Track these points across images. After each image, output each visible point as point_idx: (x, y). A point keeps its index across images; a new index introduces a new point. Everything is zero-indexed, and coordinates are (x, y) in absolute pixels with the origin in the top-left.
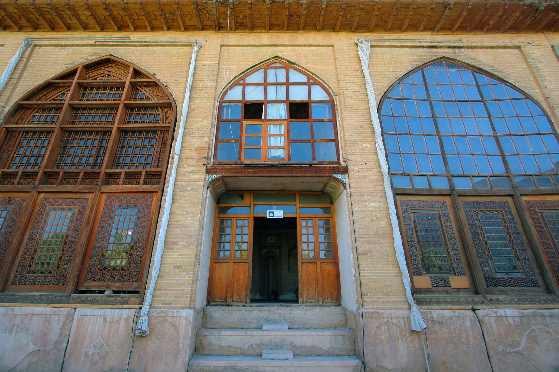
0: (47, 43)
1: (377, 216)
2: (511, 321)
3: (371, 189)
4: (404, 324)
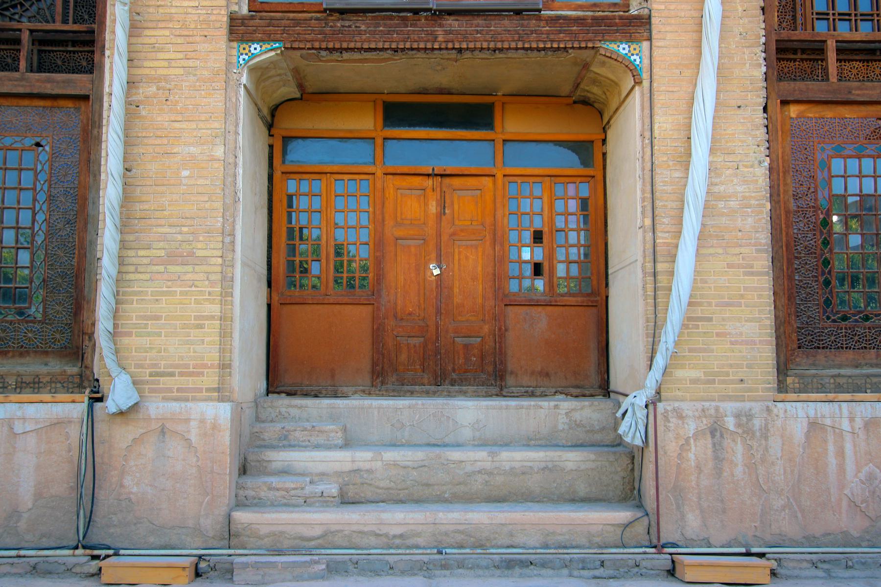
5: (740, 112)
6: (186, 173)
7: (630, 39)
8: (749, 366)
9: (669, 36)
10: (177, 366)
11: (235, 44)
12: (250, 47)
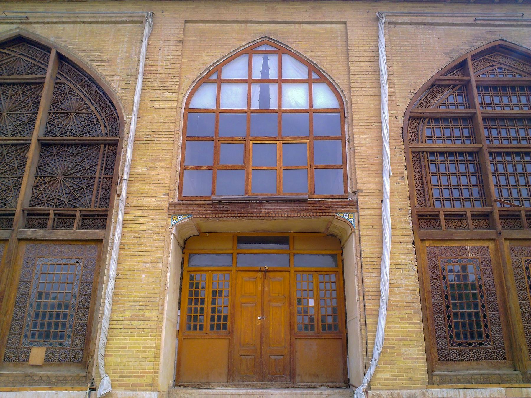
0: (406, 19)
5: (401, 245)
6: (144, 276)
7: (349, 212)
8: (413, 371)
9: (366, 210)
10: (132, 373)
11: (171, 216)
12: (177, 217)
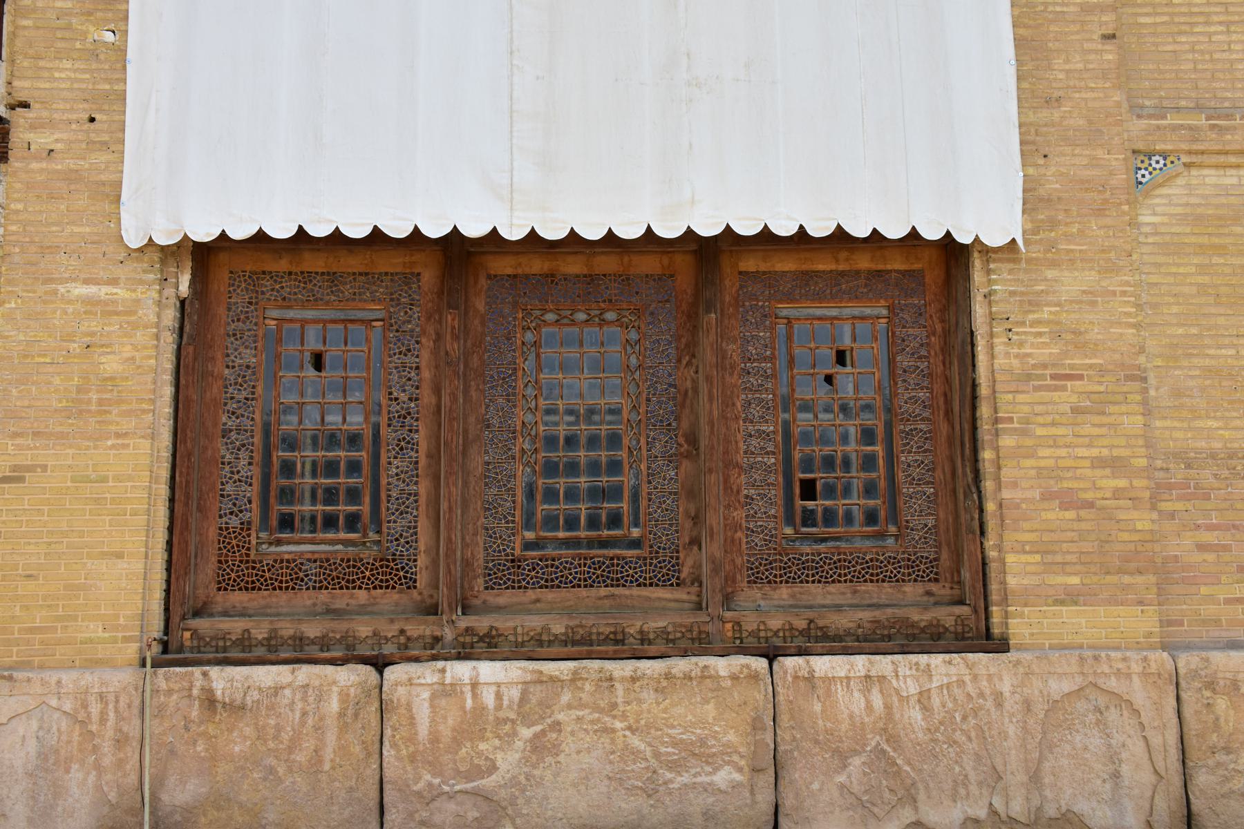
1: (93, 334)
2: (489, 698)
3: (88, 230)
4: (102, 713)
